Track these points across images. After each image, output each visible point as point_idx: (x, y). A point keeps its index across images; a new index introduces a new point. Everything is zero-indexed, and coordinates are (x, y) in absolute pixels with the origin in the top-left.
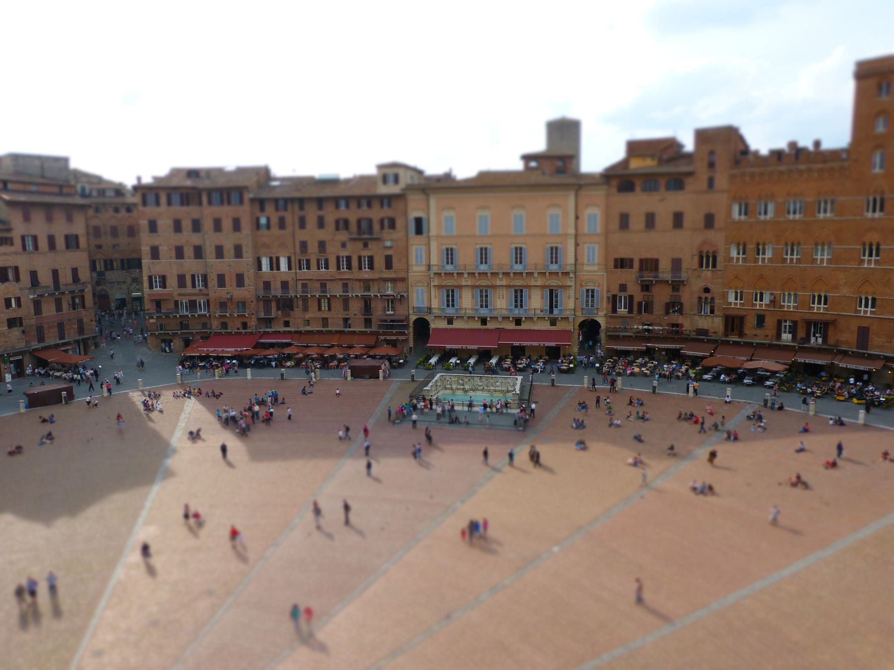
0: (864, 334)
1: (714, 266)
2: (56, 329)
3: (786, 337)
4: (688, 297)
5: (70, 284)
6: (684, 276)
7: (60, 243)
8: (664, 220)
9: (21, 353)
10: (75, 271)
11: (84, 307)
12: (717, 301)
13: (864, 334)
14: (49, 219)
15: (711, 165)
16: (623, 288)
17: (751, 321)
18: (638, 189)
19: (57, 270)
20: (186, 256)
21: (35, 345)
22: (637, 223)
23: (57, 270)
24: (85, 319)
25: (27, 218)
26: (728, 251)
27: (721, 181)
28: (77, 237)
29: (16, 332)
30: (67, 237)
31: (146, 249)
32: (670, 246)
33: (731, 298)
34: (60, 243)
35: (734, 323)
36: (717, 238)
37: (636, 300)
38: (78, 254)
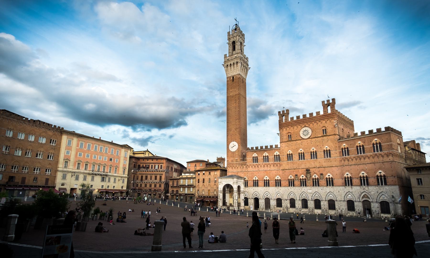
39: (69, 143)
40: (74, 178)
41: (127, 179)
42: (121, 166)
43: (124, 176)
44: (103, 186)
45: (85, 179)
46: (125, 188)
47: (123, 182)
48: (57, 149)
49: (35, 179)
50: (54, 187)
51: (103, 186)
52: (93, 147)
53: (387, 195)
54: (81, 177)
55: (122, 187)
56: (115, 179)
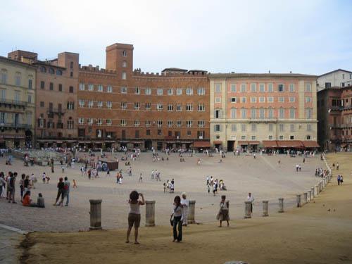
0: (124, 132)
1: (73, 108)
3: (100, 136)
4: (64, 120)
6: (63, 112)
8: (56, 87)
12: (75, 122)
13: (124, 132)
15: (72, 67)
16: (42, 115)
17: (87, 131)
18: (47, 71)
22: (47, 86)
26: (78, 102)
27: (76, 74)
32: (59, 98)
33: (80, 122)
35: (81, 131)
36: (74, 96)
37: (47, 121)
39: (218, 89)
40: (229, 130)
41: (316, 125)
42: (301, 105)
43: (310, 120)
44: (271, 137)
45: (244, 129)
46: (314, 138)
47: (309, 129)
48: (207, 98)
49: (189, 133)
50: (209, 141)
51: (271, 137)
52: (249, 88)
54: (239, 126)
55: (309, 137)
56: (292, 127)
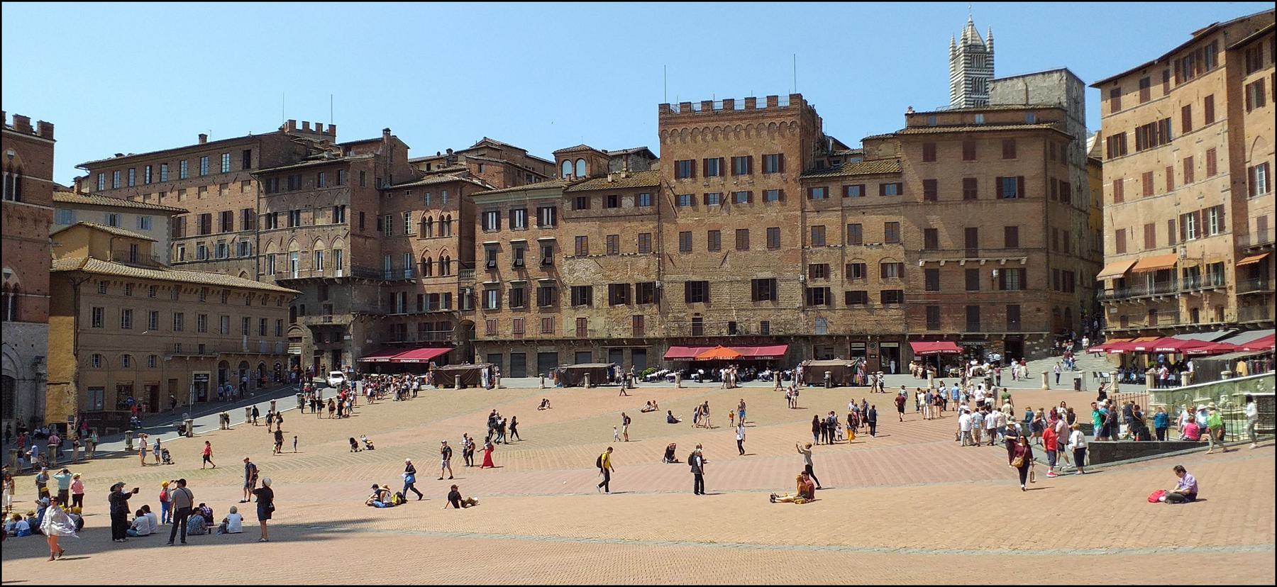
2: (963, 315)
5: (999, 250)
7: (987, 188)
9: (901, 338)
10: (1011, 235)
11: (1023, 285)
14: (969, 154)
19: (975, 230)
20: (1156, 188)
21: (923, 331)
23: (975, 230)
24: (1023, 307)
25: (930, 156)
28: (1021, 179)
29: (894, 311)
30: (1000, 181)
31: (1108, 186)
34: (987, 188)
38: (1020, 206)
53: (14, 355)
